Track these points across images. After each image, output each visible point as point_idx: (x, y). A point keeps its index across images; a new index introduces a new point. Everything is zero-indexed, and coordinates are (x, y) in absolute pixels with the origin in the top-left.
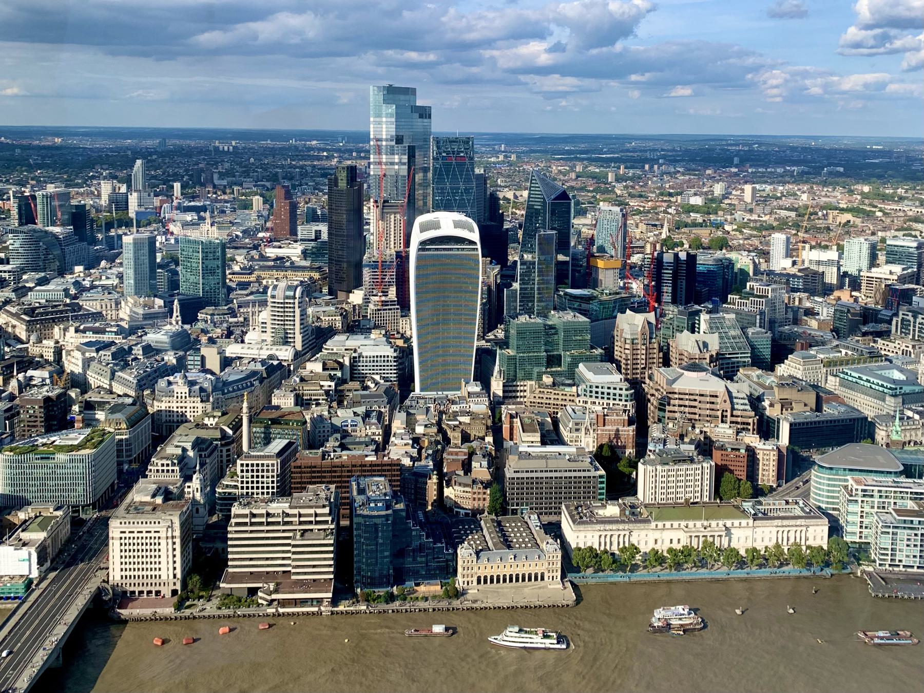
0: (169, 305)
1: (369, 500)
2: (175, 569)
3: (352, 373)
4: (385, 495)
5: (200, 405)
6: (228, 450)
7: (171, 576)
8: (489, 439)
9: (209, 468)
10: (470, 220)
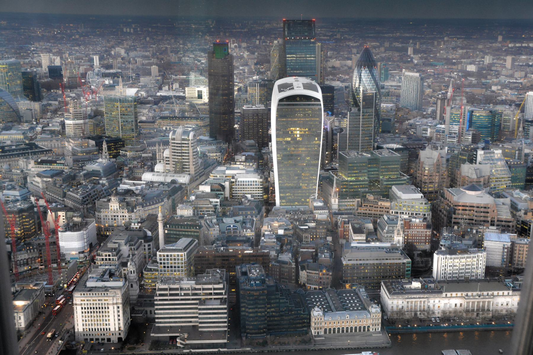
1: (250, 280)
2: (119, 324)
3: (231, 193)
5: (127, 215)
7: (117, 329)
8: (329, 239)
10: (314, 82)
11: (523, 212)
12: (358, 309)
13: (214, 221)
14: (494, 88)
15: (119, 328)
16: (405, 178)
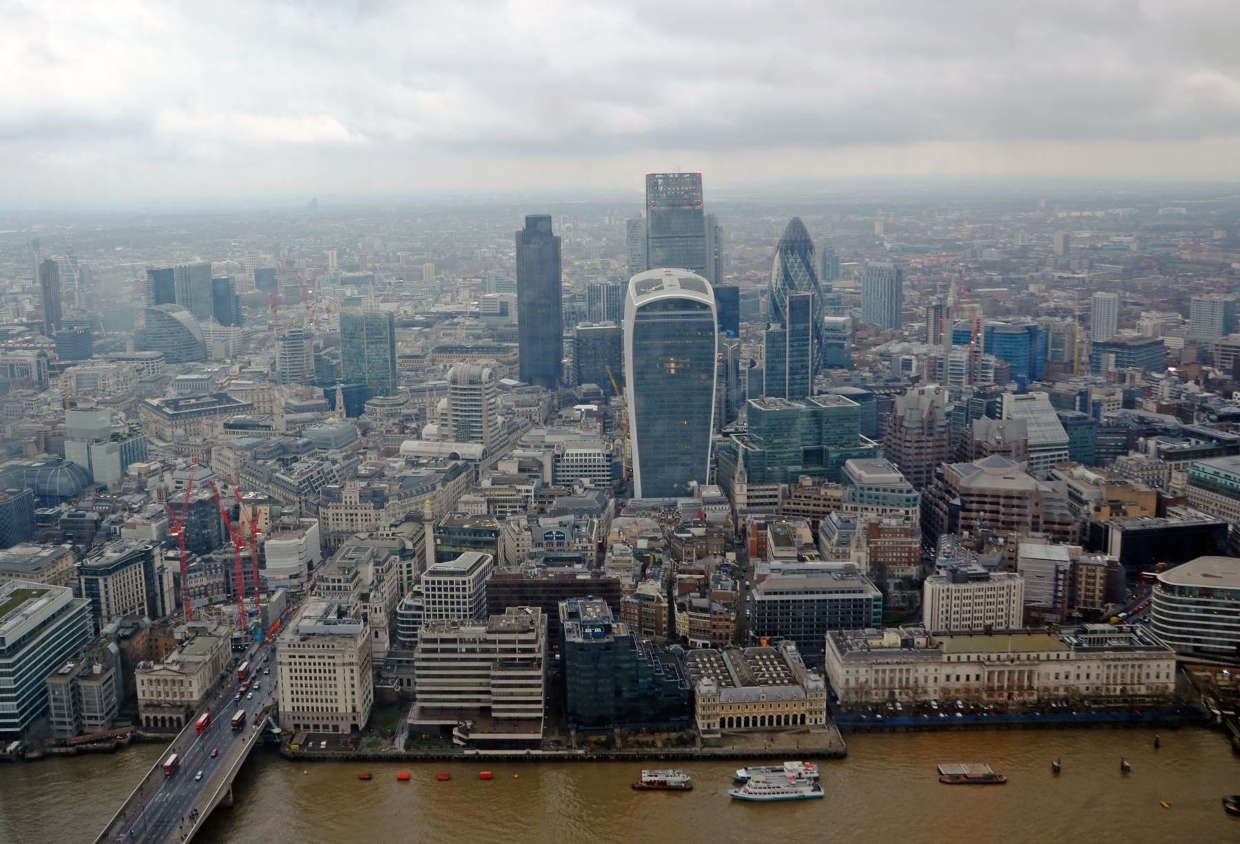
0: (330, 395)
4: (604, 618)
5: (372, 512)
6: (409, 566)
8: (731, 557)
9: (388, 585)
11: (1092, 506)
12: (782, 683)
13: (524, 522)
14: (1032, 288)
15: (354, 709)
16: (870, 446)
